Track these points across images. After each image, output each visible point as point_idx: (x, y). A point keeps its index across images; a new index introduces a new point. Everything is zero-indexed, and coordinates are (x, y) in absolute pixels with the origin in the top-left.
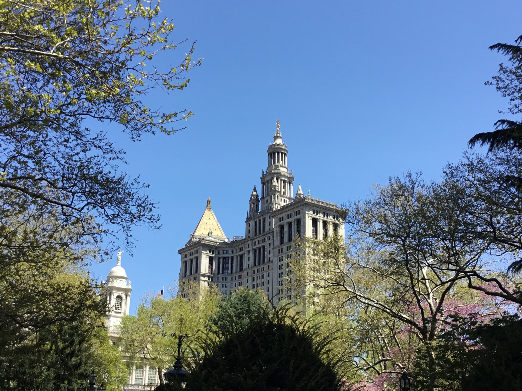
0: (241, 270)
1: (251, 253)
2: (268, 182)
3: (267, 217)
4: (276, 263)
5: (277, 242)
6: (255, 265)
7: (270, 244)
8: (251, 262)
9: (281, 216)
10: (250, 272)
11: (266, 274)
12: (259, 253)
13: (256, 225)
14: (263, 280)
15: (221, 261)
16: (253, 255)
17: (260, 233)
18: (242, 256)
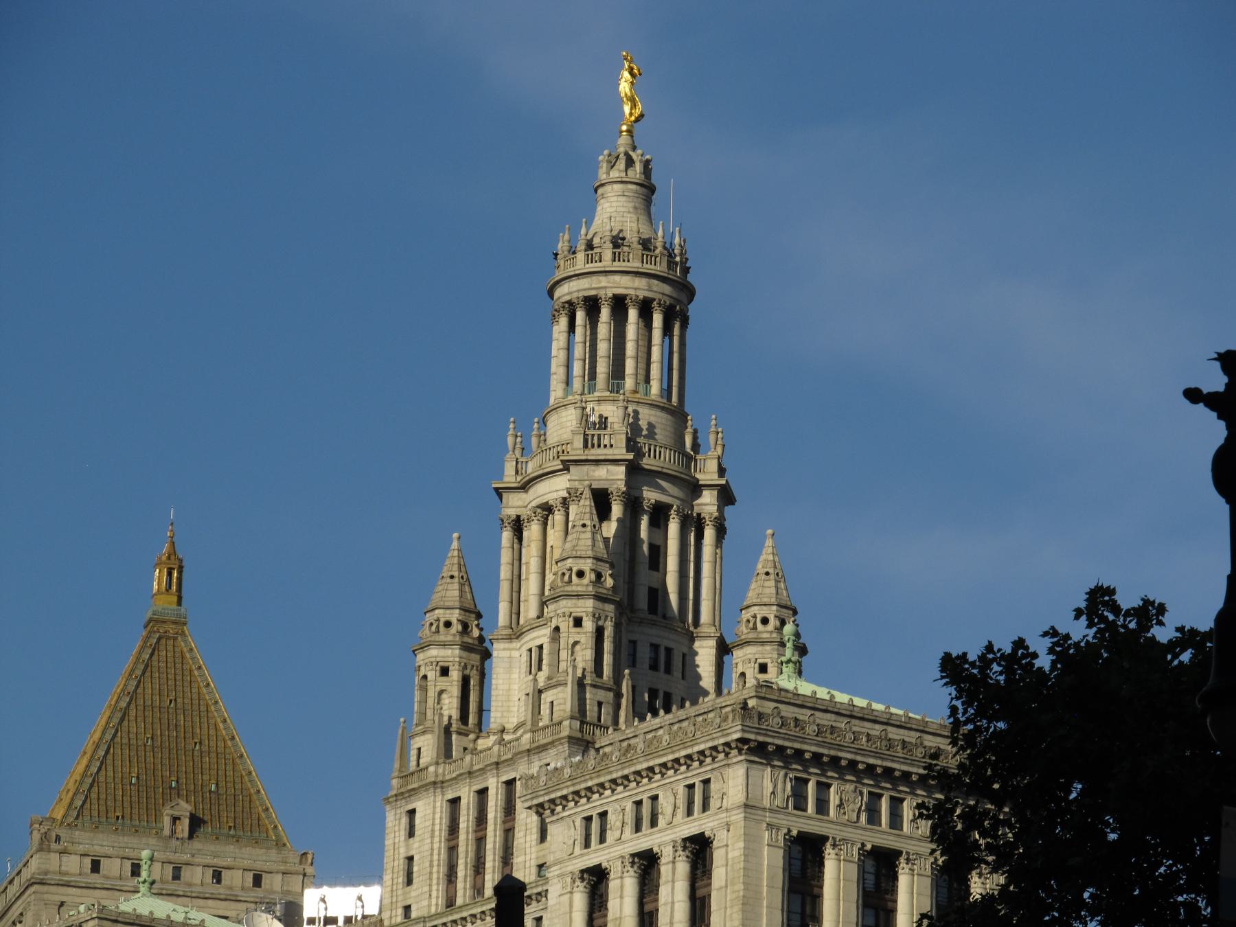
13: (453, 829)
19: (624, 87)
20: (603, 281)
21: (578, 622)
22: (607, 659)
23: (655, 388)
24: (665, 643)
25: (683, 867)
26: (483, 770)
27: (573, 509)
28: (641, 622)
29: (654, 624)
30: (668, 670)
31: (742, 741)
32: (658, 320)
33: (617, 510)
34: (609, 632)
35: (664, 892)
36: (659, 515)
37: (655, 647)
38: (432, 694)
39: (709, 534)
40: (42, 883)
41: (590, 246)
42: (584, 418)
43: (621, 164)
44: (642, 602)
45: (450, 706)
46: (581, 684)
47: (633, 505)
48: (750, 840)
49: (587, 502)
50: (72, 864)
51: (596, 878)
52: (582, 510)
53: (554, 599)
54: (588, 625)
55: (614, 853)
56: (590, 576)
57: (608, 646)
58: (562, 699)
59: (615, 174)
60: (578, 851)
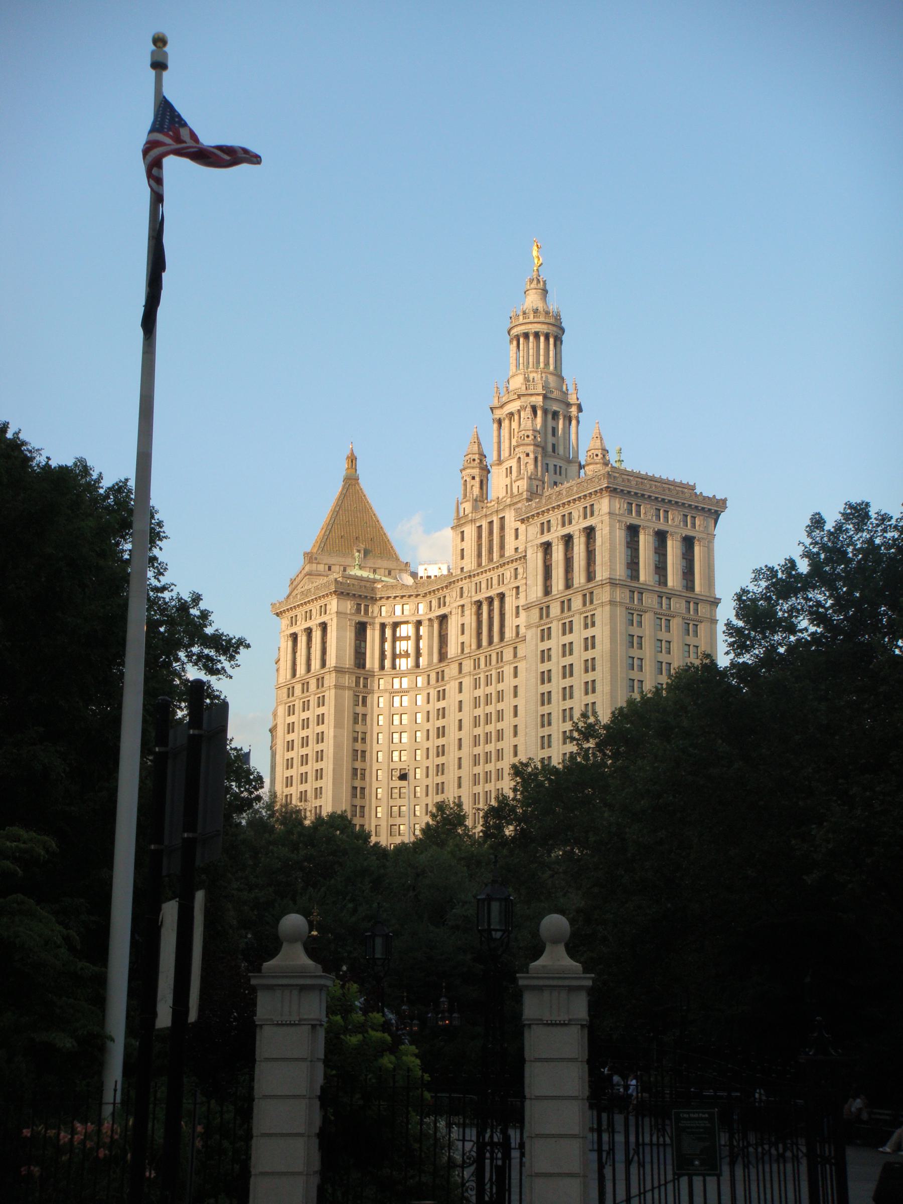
0: (443, 656)
1: (467, 613)
2: (511, 414)
3: (510, 517)
4: (530, 647)
5: (536, 591)
6: (479, 646)
7: (518, 588)
8: (469, 638)
9: (544, 519)
10: (468, 665)
11: (508, 670)
12: (490, 611)
13: (480, 537)
14: (500, 687)
15: (388, 632)
16: (474, 618)
17: (491, 560)
18: (443, 619)
19: (535, 253)
20: (530, 326)
21: (528, 455)
22: (539, 469)
23: (552, 367)
24: (559, 465)
25: (583, 539)
26: (491, 514)
27: (522, 413)
28: (550, 456)
29: (554, 457)
30: (560, 474)
31: (607, 487)
32: (552, 341)
33: (539, 413)
34: (539, 458)
35: (576, 549)
36: (555, 415)
37: (555, 466)
38: (468, 486)
39: (574, 422)
40: (310, 575)
41: (524, 313)
42: (527, 380)
43: (535, 282)
44: (550, 449)
45: (476, 491)
46: (530, 478)
47: (545, 412)
48: (611, 526)
49: (529, 410)
50: (321, 567)
51: (547, 547)
52: (526, 414)
53: (518, 446)
54: (532, 456)
55: (555, 535)
56: (531, 437)
57: (539, 464)
58: (523, 484)
59: (532, 286)
60: (539, 536)
